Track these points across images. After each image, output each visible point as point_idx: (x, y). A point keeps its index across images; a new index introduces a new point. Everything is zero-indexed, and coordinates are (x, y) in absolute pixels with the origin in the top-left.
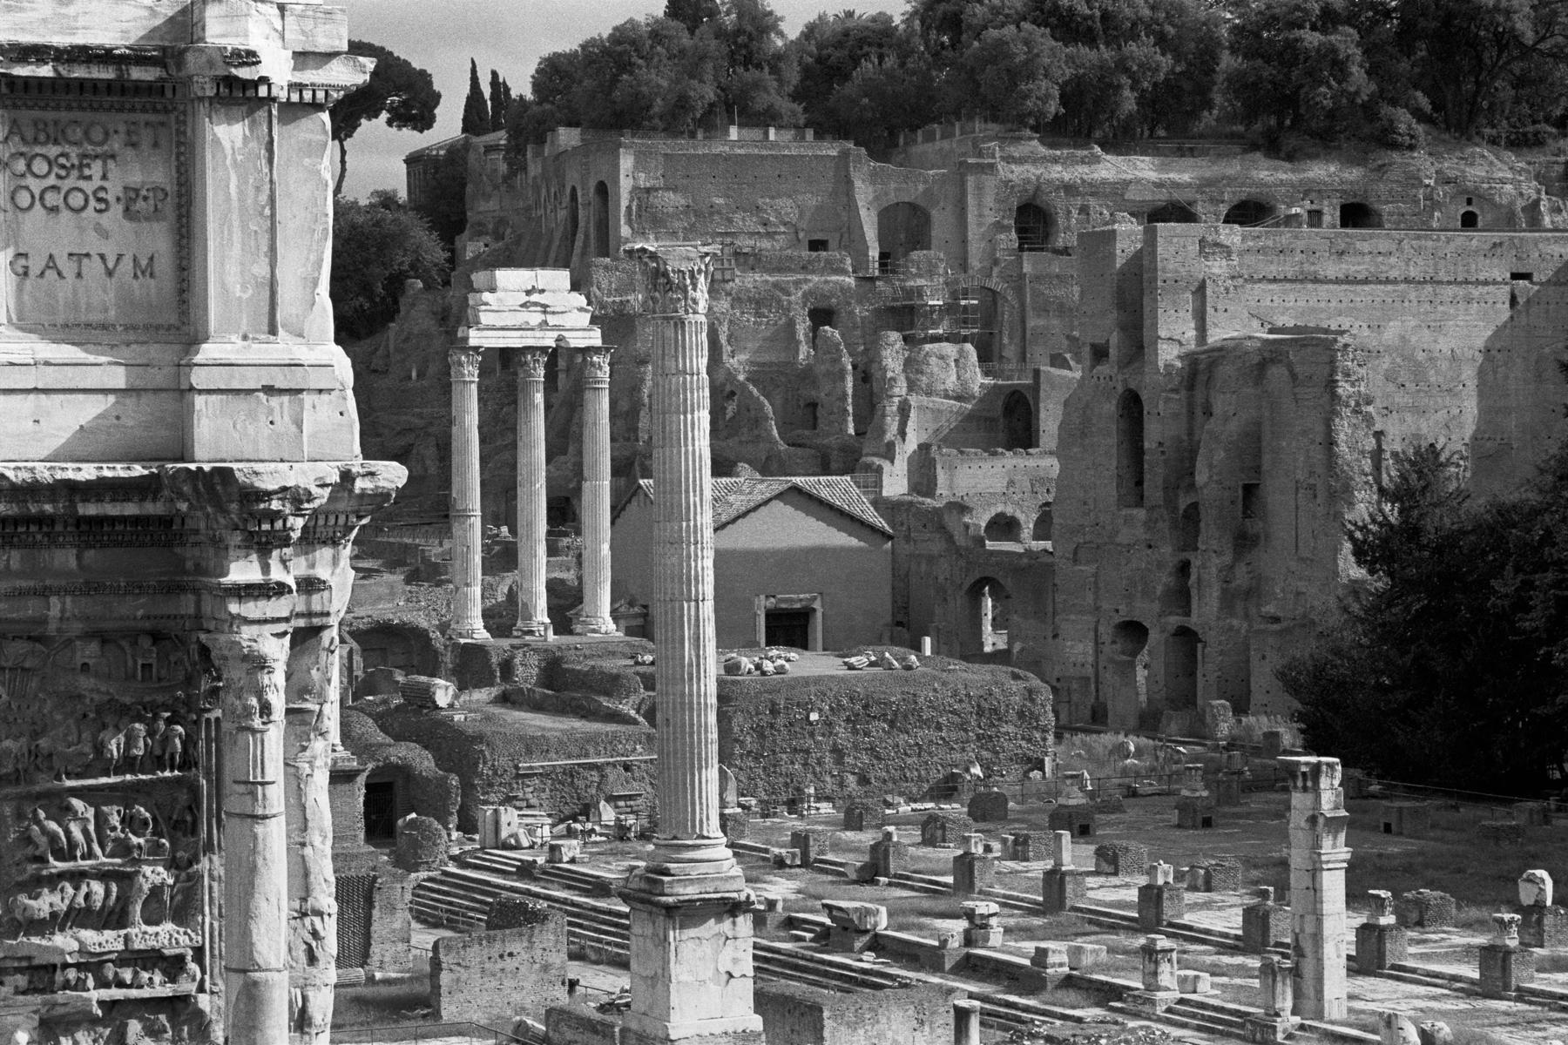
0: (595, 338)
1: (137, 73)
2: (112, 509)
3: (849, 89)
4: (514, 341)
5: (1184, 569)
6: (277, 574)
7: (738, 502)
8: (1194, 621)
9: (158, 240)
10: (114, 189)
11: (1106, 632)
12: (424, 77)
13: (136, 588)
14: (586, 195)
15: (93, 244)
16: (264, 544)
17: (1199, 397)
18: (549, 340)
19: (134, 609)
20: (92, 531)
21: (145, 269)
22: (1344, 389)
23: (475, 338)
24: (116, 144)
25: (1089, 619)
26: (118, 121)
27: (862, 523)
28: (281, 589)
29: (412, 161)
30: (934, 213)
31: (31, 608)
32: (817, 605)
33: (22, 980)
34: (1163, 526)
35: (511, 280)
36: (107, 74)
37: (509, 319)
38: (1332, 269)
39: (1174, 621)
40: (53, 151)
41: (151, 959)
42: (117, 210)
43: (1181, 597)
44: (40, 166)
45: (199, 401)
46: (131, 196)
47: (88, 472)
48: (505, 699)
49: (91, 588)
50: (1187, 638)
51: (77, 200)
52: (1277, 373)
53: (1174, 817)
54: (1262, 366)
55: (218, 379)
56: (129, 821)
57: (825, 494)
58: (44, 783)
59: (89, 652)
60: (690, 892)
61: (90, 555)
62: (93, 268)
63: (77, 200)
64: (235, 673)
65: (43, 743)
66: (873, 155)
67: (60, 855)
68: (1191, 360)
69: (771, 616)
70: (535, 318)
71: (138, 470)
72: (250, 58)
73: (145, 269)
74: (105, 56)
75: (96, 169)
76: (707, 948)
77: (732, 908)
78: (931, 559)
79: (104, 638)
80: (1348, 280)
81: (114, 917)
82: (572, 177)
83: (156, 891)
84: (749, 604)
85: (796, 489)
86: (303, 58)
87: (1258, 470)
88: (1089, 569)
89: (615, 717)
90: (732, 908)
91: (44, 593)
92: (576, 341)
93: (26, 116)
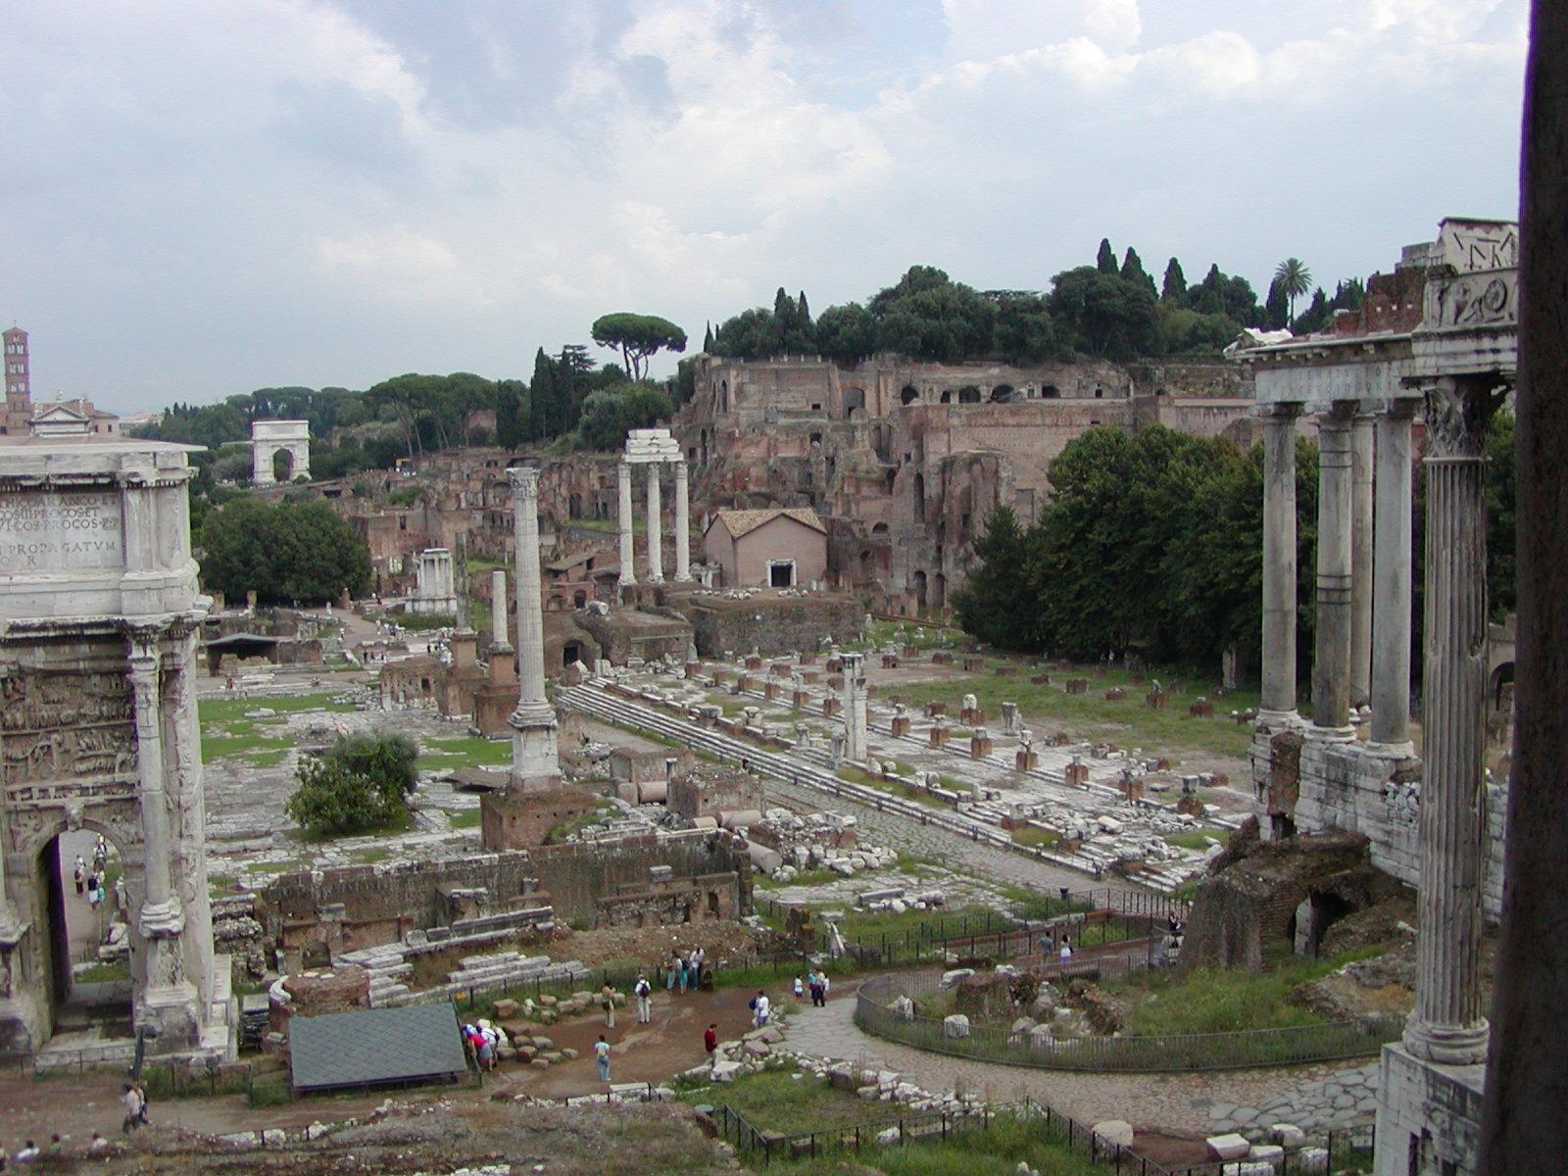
0: (681, 457)
1: (101, 481)
2: (96, 632)
3: (838, 338)
4: (645, 459)
5: (939, 549)
6: (149, 654)
7: (759, 521)
8: (944, 571)
9: (114, 536)
10: (99, 520)
11: (911, 577)
12: (680, 330)
13: (109, 658)
14: (719, 385)
15: (92, 539)
16: (144, 645)
17: (947, 476)
18: (660, 459)
19: (110, 665)
20: (92, 639)
21: (110, 547)
22: (1003, 474)
23: (628, 458)
24: (99, 504)
25: (905, 570)
26: (99, 496)
27: (813, 529)
28: (151, 660)
29: (681, 364)
30: (867, 392)
31: (73, 666)
32: (794, 564)
33: (78, 792)
34: (932, 531)
35: (643, 434)
36: (91, 481)
37: (643, 451)
38: (1011, 421)
39: (936, 571)
40: (76, 507)
41: (123, 785)
42: (100, 527)
43: (939, 560)
44: (72, 513)
45: (124, 594)
46: (105, 521)
47: (86, 620)
48: (639, 609)
49: (93, 659)
50: (941, 578)
51: (85, 524)
52: (977, 468)
53: (881, 663)
54: (971, 464)
55: (130, 586)
56: (113, 736)
57: (800, 517)
58: (83, 724)
59: (96, 679)
60: (529, 723)
61: (94, 647)
62: (92, 547)
63: (85, 524)
64: (138, 690)
65: (82, 711)
66: (842, 367)
67: (89, 748)
68: (944, 460)
69: (773, 568)
70: (654, 450)
71: (104, 618)
72: (135, 474)
73: (110, 547)
74: (89, 476)
75: (92, 513)
76: (537, 745)
77: (548, 728)
78: (847, 543)
79: (103, 674)
80: (1019, 425)
81: (111, 770)
82: (714, 379)
83: (123, 763)
84: (764, 564)
85: (783, 515)
86: (163, 470)
87: (969, 508)
88: (904, 549)
89: (675, 618)
90: (548, 728)
91: (77, 660)
92: (672, 459)
93: (67, 497)
